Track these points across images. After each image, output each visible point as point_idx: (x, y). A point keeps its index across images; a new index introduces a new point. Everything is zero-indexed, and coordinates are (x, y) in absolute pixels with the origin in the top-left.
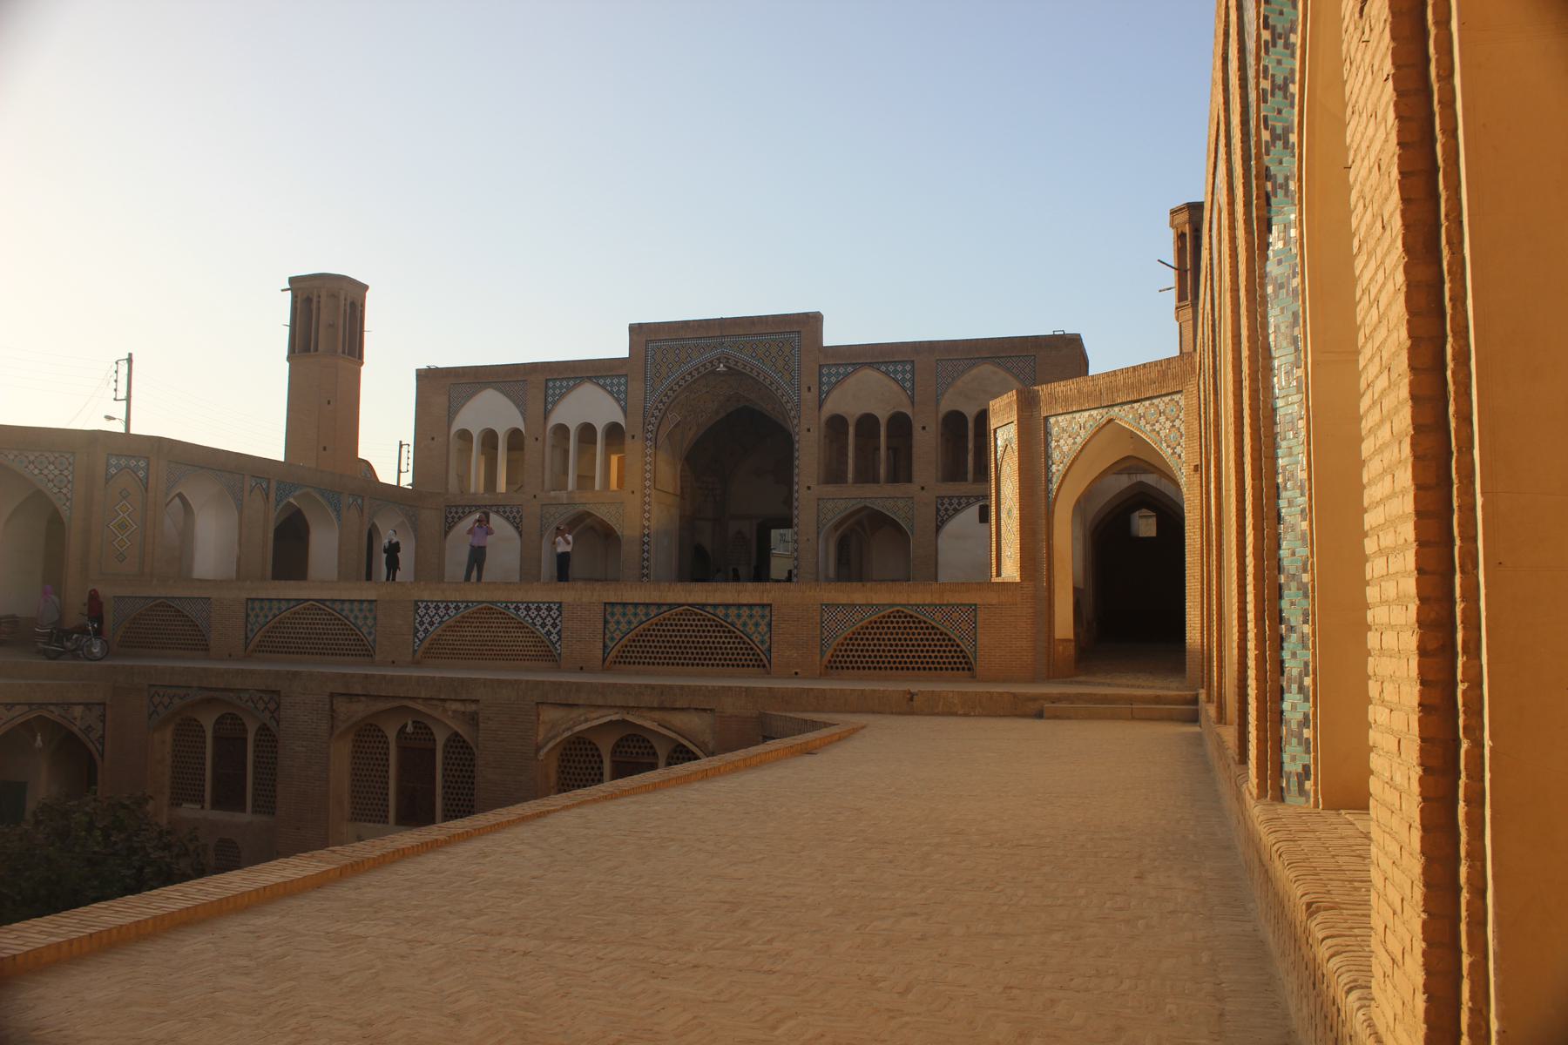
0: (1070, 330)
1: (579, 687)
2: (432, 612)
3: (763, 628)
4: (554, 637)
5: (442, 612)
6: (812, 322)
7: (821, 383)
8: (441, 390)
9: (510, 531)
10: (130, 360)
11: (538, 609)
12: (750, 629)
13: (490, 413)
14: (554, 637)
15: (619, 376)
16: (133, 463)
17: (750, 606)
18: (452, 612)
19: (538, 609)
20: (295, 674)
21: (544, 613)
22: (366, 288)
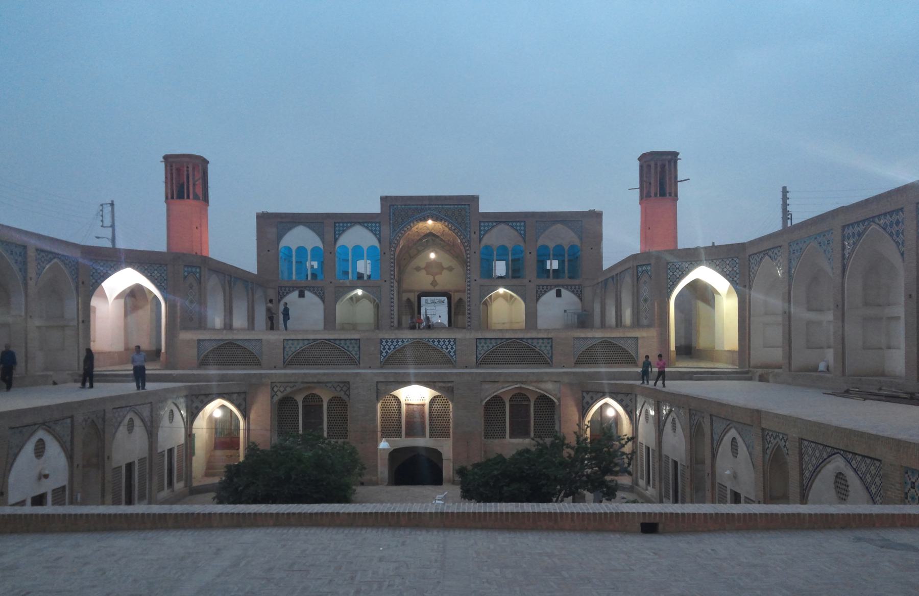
0: (597, 209)
1: (500, 374)
2: (390, 343)
3: (549, 348)
4: (452, 354)
5: (395, 343)
6: (475, 199)
7: (480, 230)
8: (272, 226)
9: (317, 300)
10: (112, 204)
11: (444, 341)
12: (543, 348)
13: (301, 238)
14: (452, 354)
15: (376, 223)
16: (194, 270)
17: (543, 339)
18: (400, 343)
19: (444, 341)
20: (357, 374)
21: (447, 343)
22: (207, 162)
